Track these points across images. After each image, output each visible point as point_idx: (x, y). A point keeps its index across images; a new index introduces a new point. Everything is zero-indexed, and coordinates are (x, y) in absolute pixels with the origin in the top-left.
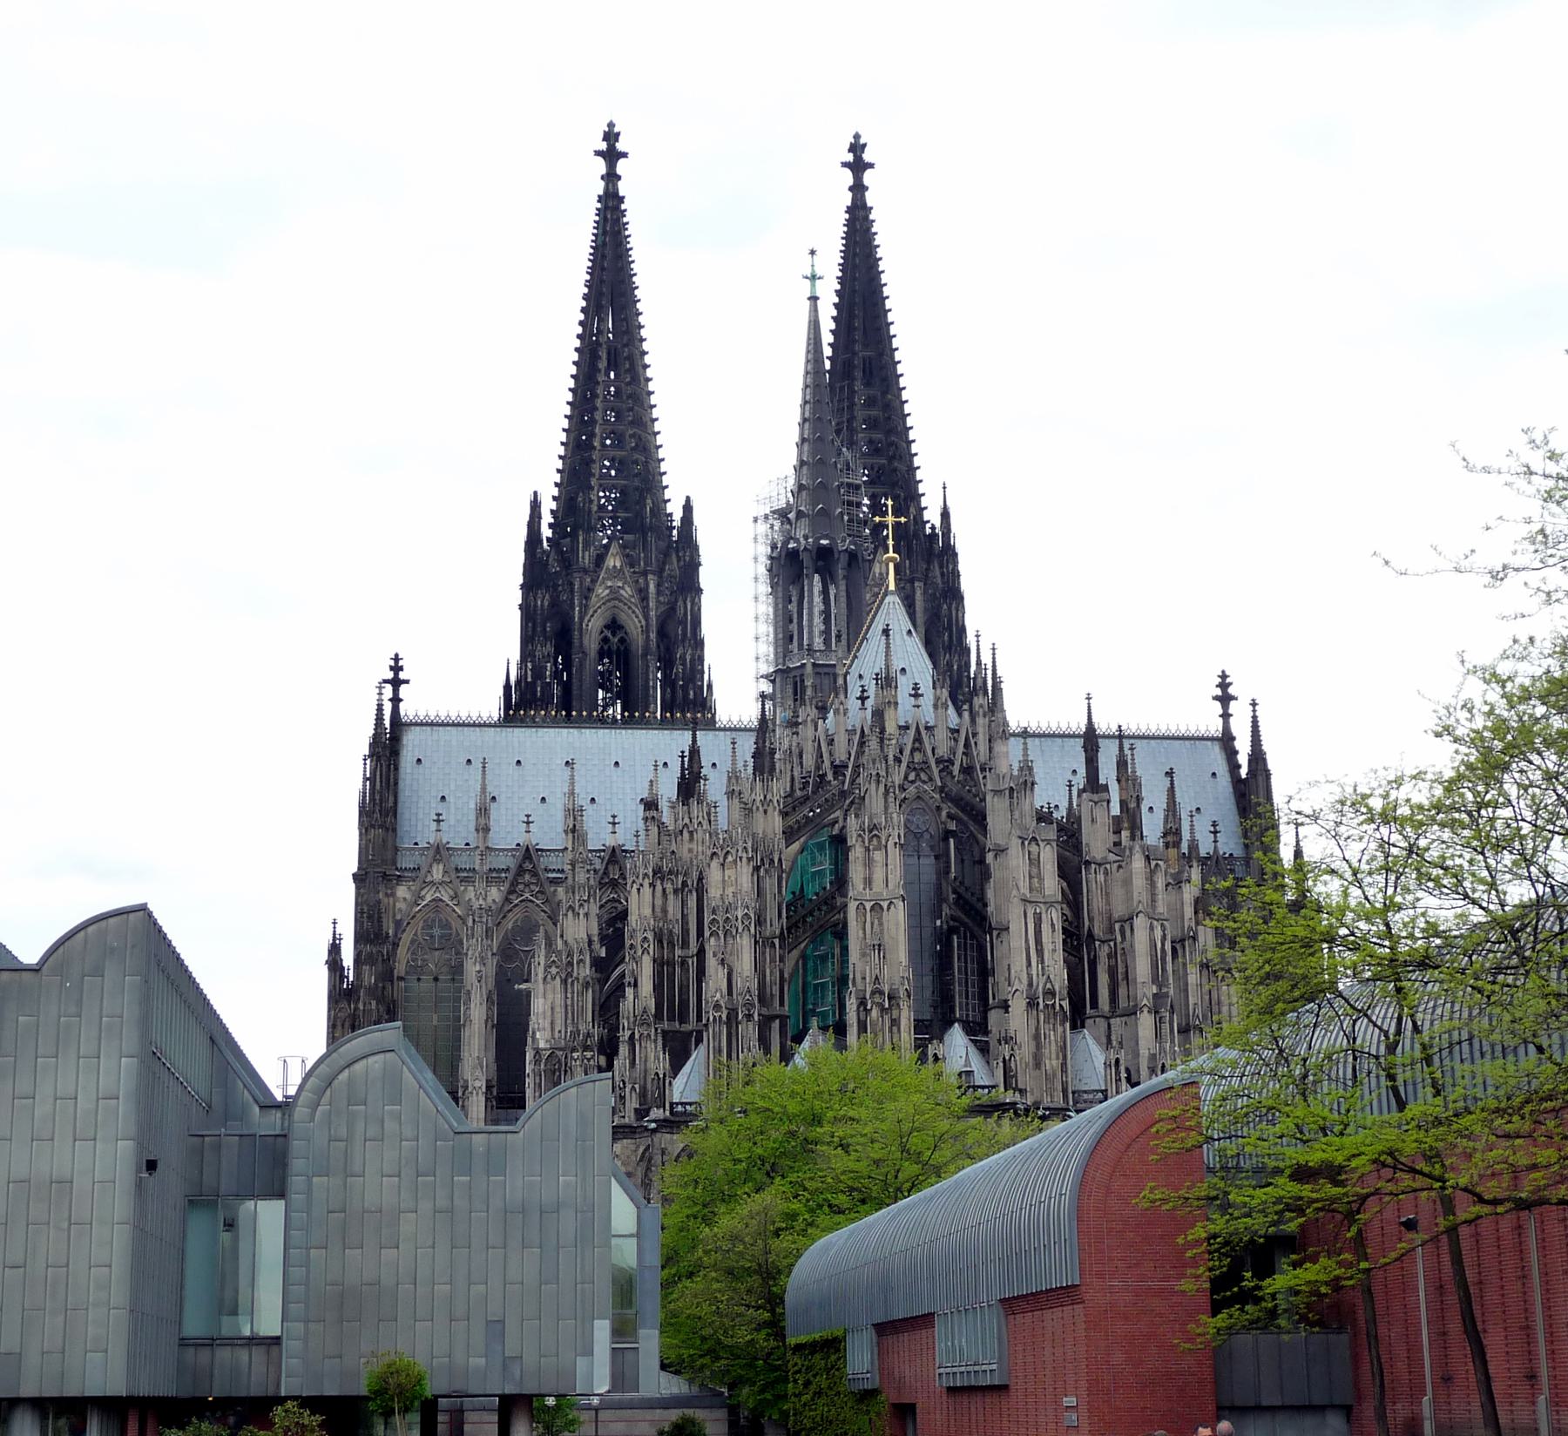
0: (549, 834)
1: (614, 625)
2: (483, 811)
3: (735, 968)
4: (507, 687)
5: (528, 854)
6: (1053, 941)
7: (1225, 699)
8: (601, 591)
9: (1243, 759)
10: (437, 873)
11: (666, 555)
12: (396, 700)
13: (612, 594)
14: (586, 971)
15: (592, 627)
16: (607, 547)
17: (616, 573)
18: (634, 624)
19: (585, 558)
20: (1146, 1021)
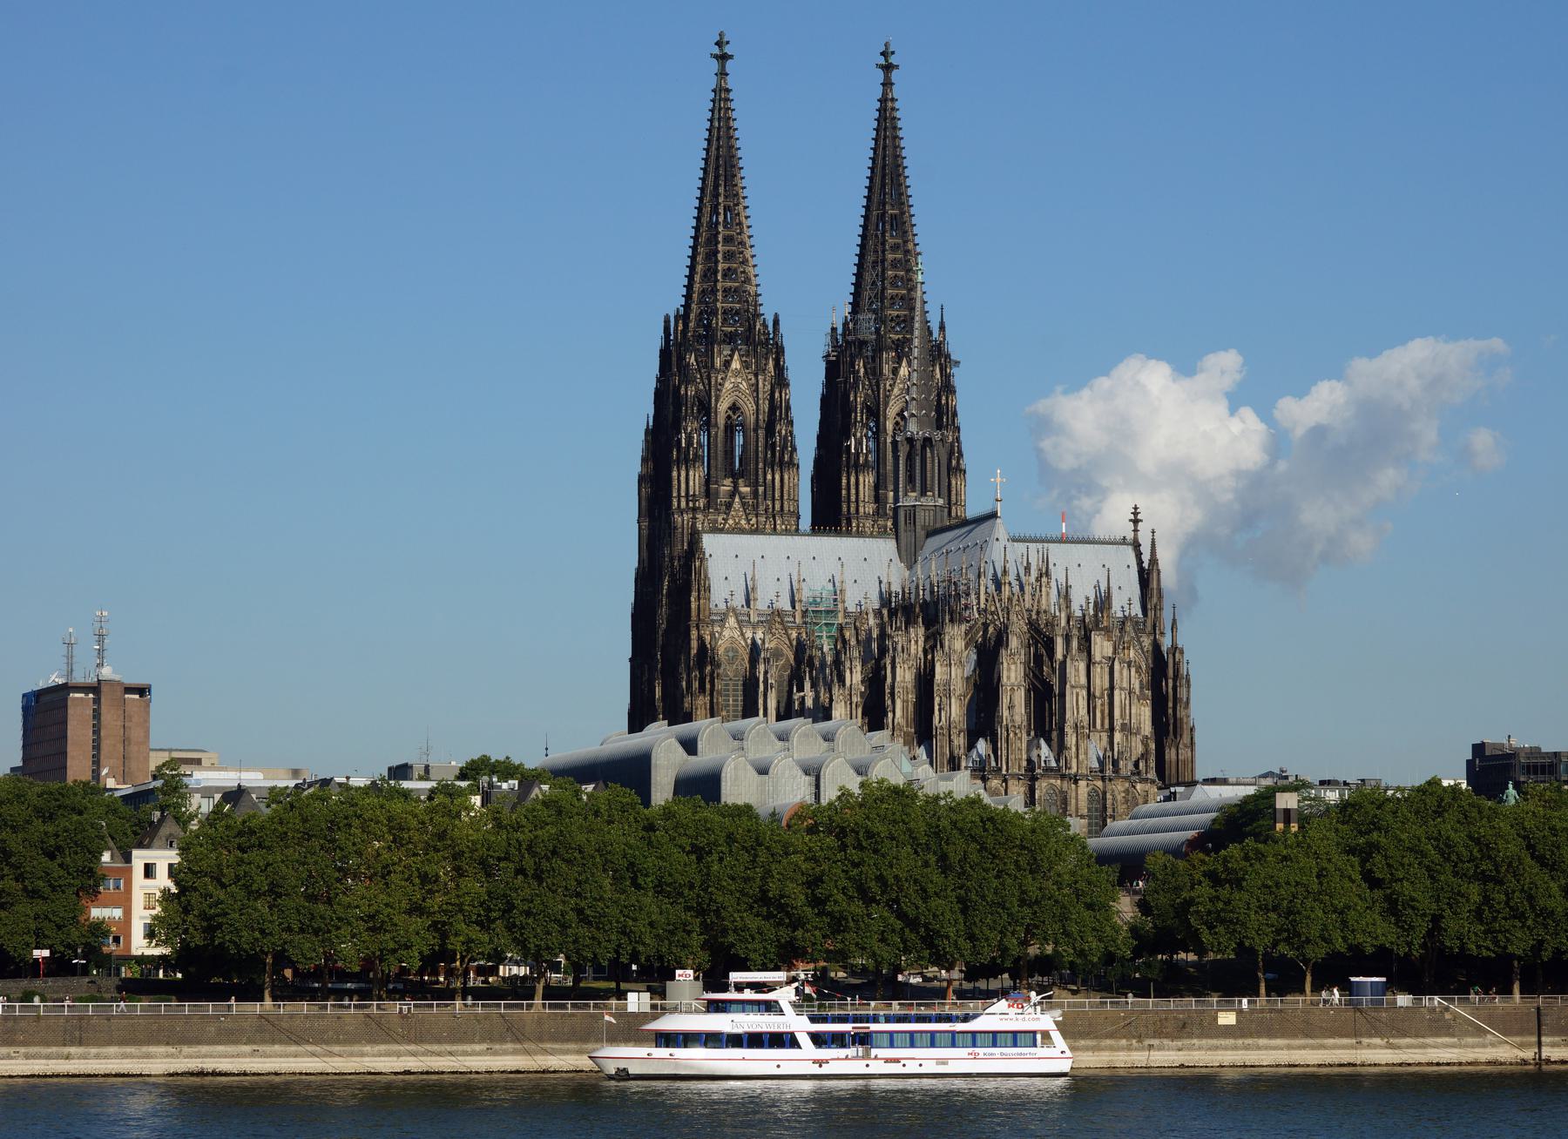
1: (734, 408)
7: (1136, 522)
8: (728, 385)
9: (1146, 558)
10: (732, 621)
16: (732, 356)
17: (737, 373)
18: (749, 407)
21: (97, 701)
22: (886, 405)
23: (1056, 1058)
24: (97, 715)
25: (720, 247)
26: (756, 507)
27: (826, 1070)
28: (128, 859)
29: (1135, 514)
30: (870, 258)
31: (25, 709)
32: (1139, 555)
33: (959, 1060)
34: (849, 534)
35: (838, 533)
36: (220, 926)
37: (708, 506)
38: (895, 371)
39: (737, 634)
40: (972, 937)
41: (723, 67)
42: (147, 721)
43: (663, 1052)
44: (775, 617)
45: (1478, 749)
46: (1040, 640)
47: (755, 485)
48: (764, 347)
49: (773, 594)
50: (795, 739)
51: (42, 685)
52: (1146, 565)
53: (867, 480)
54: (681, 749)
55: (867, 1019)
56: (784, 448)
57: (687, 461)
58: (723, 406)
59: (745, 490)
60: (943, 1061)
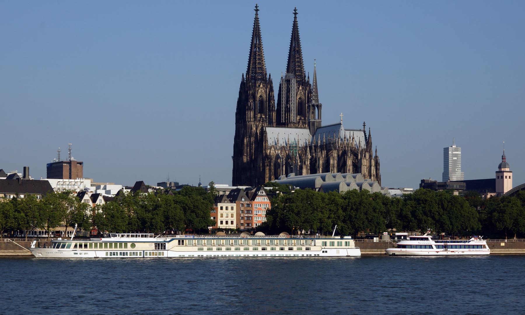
1: (261, 96)
8: (260, 91)
18: (264, 96)
21: (70, 166)
23: (486, 251)
24: (70, 169)
27: (439, 254)
28: (217, 205)
30: (291, 60)
31: (47, 168)
32: (365, 134)
33: (467, 252)
34: (288, 127)
35: (285, 127)
36: (287, 221)
37: (255, 121)
40: (451, 224)
42: (82, 171)
43: (399, 249)
44: (282, 148)
45: (423, 181)
46: (355, 154)
48: (268, 83)
49: (282, 143)
50: (347, 177)
51: (52, 162)
52: (367, 136)
53: (252, 113)
54: (322, 180)
55: (447, 242)
56: (273, 107)
57: (250, 109)
58: (258, 96)
59: (263, 116)
60: (463, 252)
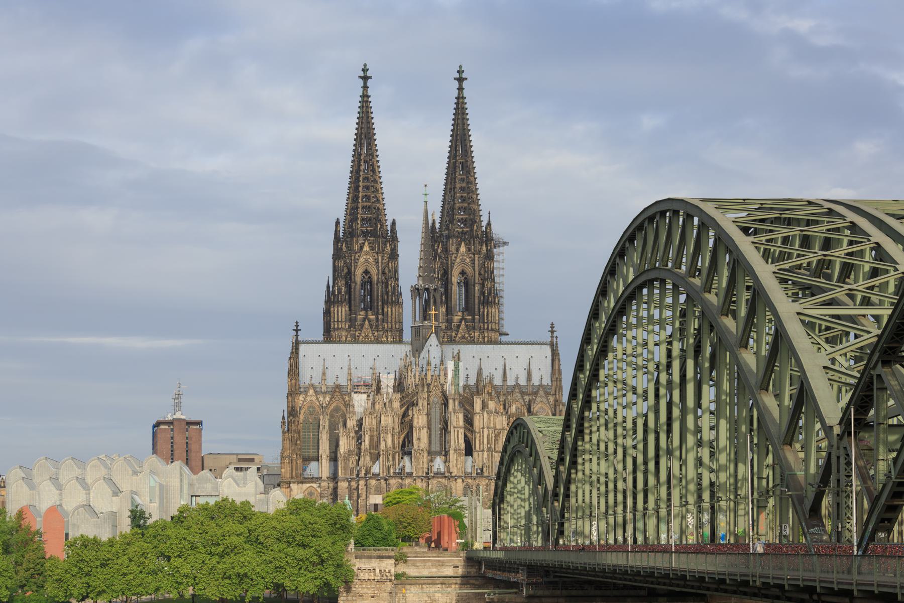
0: (343, 381)
1: (366, 272)
2: (324, 374)
3: (388, 442)
4: (328, 287)
5: (338, 387)
6: (461, 437)
7: (552, 332)
8: (362, 260)
10: (311, 392)
11: (386, 244)
12: (297, 335)
13: (366, 260)
14: (352, 434)
15: (359, 273)
17: (367, 253)
18: (374, 272)
19: (356, 247)
20: (485, 453)
22: (452, 267)
25: (361, 184)
26: (377, 326)
29: (552, 327)
32: (553, 350)
38: (458, 249)
39: (314, 398)
41: (365, 83)
47: (377, 314)
48: (386, 239)
